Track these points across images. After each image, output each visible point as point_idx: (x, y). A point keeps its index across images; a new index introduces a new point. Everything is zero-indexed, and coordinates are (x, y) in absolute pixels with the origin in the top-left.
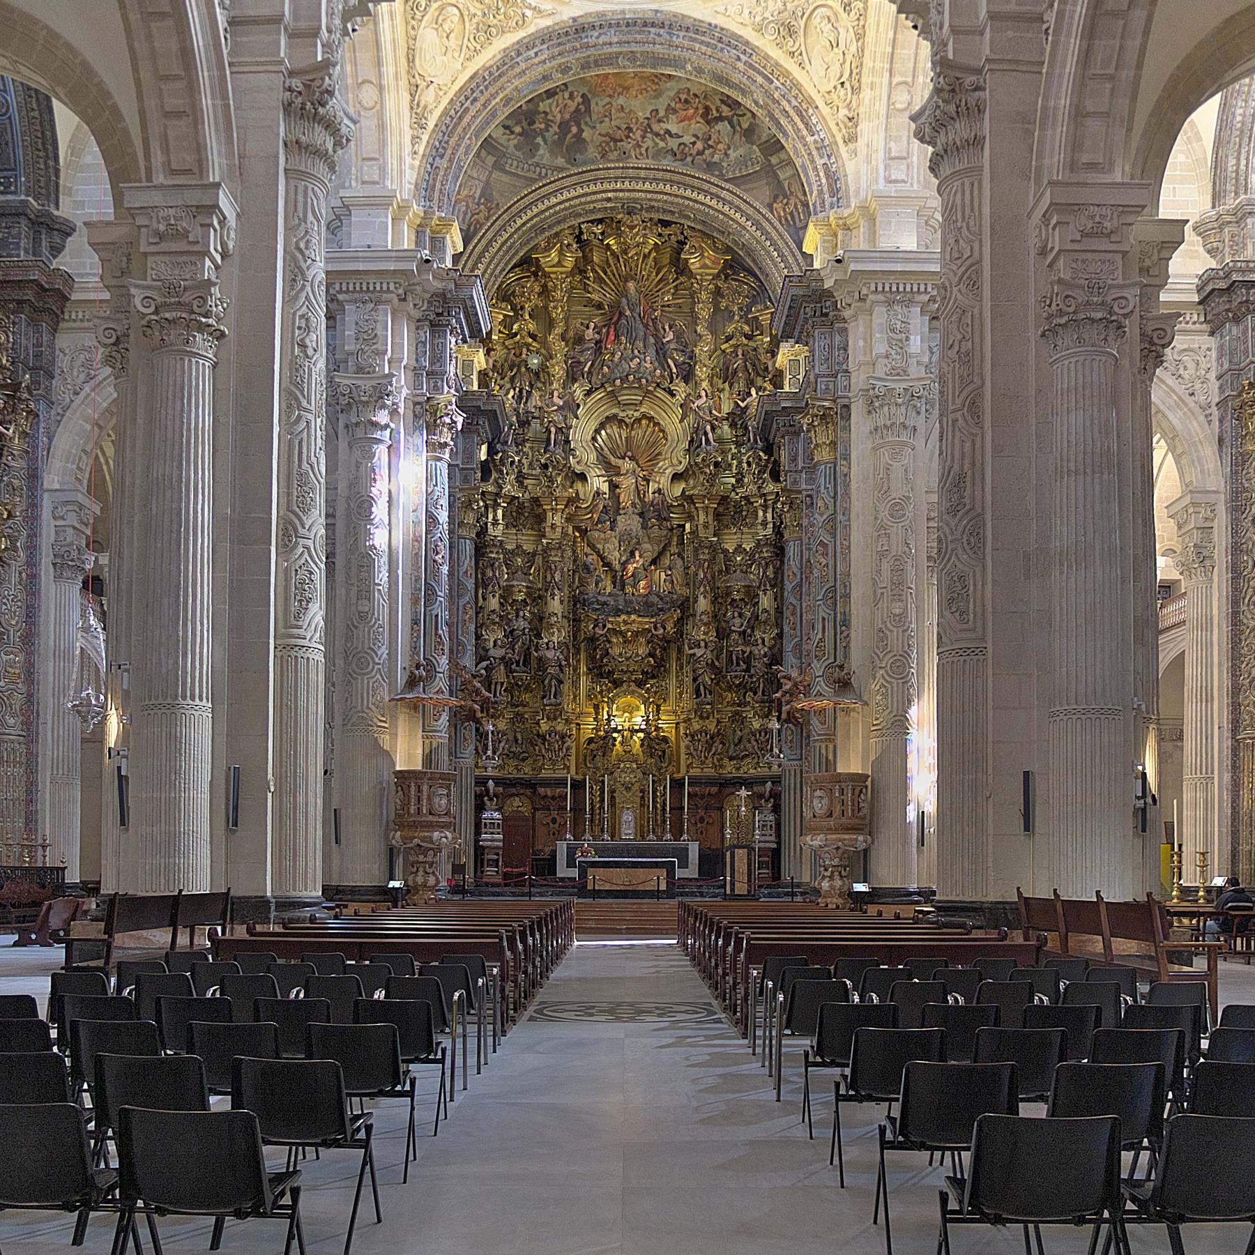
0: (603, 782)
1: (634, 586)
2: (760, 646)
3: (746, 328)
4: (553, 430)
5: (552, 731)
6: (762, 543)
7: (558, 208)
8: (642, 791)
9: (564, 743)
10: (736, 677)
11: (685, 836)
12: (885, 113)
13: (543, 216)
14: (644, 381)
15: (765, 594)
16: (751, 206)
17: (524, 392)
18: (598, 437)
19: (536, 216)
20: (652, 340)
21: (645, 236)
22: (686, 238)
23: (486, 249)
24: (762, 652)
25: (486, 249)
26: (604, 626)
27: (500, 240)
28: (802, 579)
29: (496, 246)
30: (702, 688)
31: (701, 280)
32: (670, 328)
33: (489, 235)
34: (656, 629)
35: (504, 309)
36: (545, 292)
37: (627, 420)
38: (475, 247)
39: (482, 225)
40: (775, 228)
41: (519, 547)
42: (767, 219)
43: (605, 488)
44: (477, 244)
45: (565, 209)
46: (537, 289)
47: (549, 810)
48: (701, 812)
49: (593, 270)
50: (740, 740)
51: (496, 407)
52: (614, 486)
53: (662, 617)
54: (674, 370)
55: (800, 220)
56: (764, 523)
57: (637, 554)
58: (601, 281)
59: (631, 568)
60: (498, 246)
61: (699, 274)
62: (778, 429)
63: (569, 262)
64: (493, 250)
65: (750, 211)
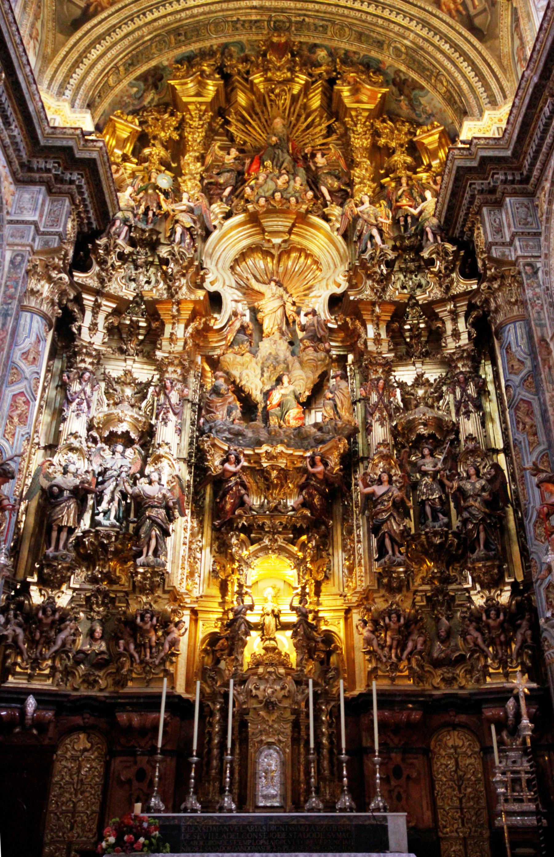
0: (226, 696)
1: (282, 417)
2: (474, 479)
3: (409, 160)
4: (179, 230)
5: (147, 611)
6: (455, 357)
7: (195, 11)
8: (296, 712)
9: (167, 633)
10: (435, 534)
11: (378, 801)
12: (521, 22)
13: (178, 17)
14: (293, 200)
15: (468, 417)
16: (416, 6)
17: (151, 214)
18: (237, 267)
19: (169, 14)
20: (301, 171)
21: (291, 70)
22: (339, 73)
23: (108, 32)
24: (478, 486)
25: (108, 32)
26: (238, 461)
27: (126, 30)
28: (535, 367)
29: (121, 33)
30: (387, 542)
31: (357, 116)
32: (323, 155)
33: (113, 21)
34: (313, 465)
35: (131, 123)
36: (180, 127)
37: (272, 251)
38: (93, 28)
39: (103, 9)
40: (444, 22)
41: (128, 373)
42: (435, 16)
43: (243, 308)
44: (96, 26)
45: (203, 13)
46: (174, 122)
47: (133, 754)
48: (396, 757)
49: (237, 113)
50: (449, 633)
51: (95, 155)
52: (254, 311)
53: (320, 449)
54: (328, 197)
55: (475, 7)
56: (456, 335)
57: (285, 379)
58: (245, 122)
59: (276, 397)
60: (123, 34)
61: (356, 109)
62: (473, 197)
63: (211, 88)
64: (115, 37)
65: (414, 11)
